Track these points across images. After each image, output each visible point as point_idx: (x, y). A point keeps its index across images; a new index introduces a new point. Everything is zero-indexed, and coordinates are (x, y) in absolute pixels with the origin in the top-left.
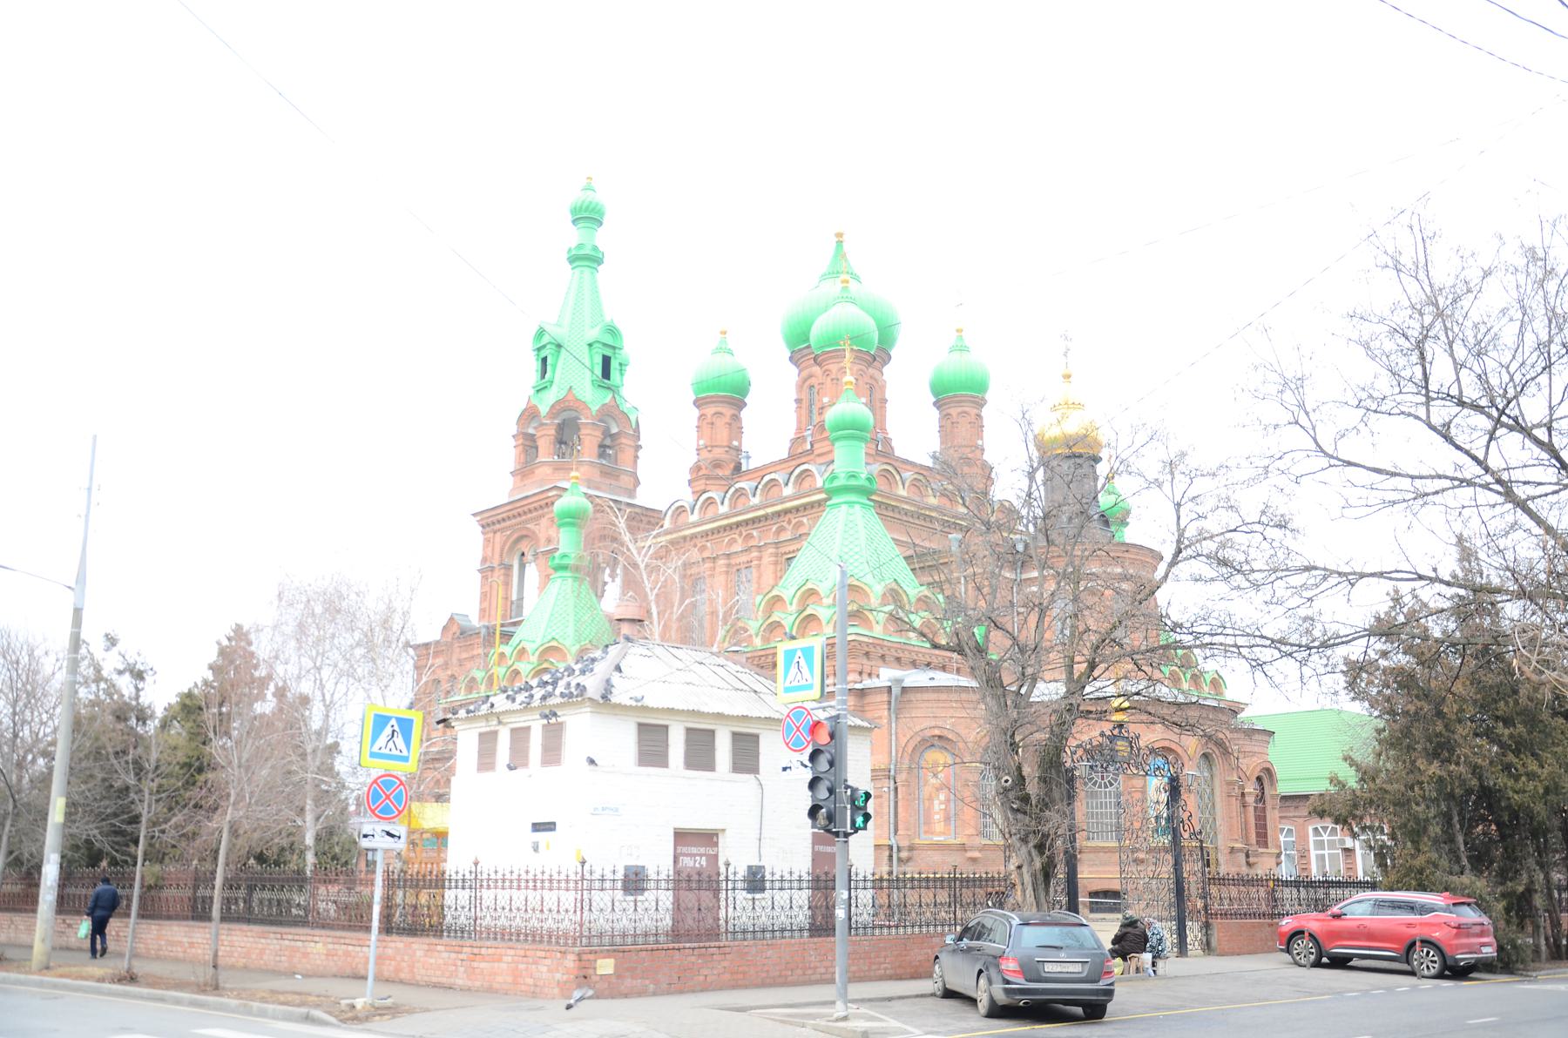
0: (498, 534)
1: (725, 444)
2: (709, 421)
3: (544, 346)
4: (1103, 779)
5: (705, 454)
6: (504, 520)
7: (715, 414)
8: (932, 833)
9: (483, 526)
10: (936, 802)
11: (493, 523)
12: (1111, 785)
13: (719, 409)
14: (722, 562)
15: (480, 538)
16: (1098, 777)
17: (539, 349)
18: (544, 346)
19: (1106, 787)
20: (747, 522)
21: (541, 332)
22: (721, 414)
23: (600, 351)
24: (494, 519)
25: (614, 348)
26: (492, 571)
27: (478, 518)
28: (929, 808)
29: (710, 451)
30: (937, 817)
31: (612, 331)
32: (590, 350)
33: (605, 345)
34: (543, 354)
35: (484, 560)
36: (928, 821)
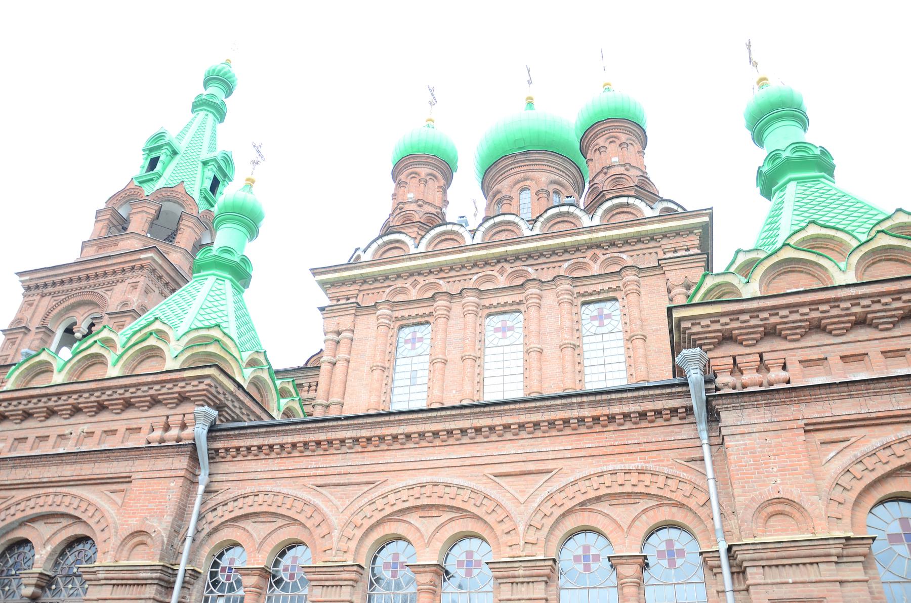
0: (47, 298)
3: (160, 147)
6: (62, 282)
7: (430, 174)
9: (28, 288)
11: (46, 285)
13: (435, 172)
14: (471, 299)
15: (20, 299)
17: (151, 150)
18: (160, 147)
20: (517, 257)
21: (160, 136)
22: (436, 177)
23: (215, 169)
24: (49, 281)
25: (225, 175)
26: (25, 334)
27: (27, 278)
29: (420, 206)
31: (227, 159)
32: (203, 168)
33: (220, 168)
34: (154, 155)
35: (18, 320)
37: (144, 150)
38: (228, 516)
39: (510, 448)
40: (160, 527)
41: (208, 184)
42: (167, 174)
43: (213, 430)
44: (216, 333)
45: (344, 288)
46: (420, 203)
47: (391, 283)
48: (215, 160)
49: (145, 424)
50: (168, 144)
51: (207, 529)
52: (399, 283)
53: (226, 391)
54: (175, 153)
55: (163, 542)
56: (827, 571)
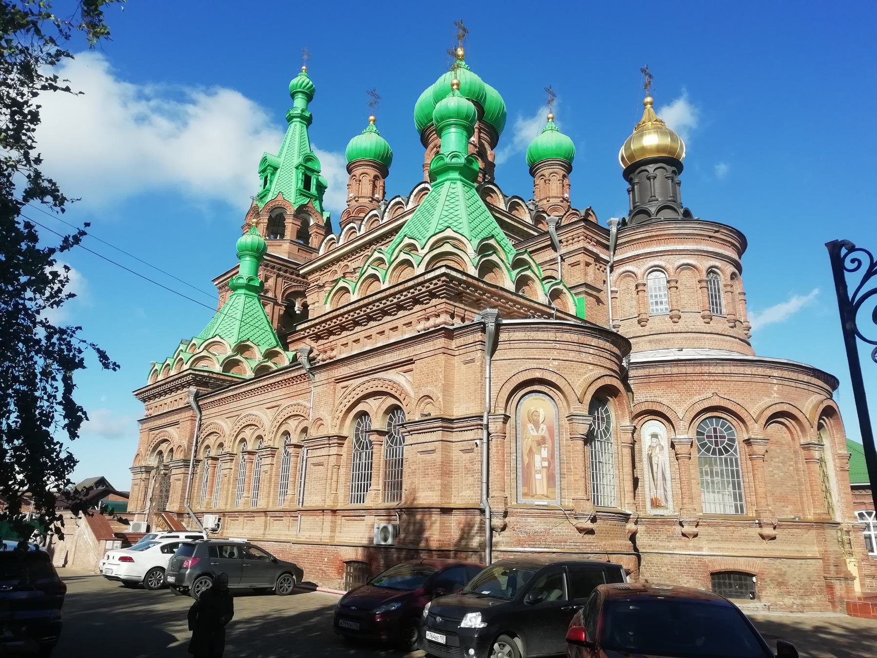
1: (369, 195)
2: (357, 178)
4: (717, 445)
5: (353, 203)
8: (533, 496)
10: (537, 458)
12: (714, 453)
16: (711, 442)
17: (264, 171)
19: (721, 453)
21: (265, 160)
28: (529, 464)
29: (357, 201)
30: (538, 476)
34: (265, 175)
36: (527, 480)
37: (260, 173)
38: (206, 434)
39: (270, 395)
40: (185, 443)
41: (301, 185)
42: (272, 190)
43: (197, 396)
44: (217, 339)
45: (314, 275)
46: (357, 199)
47: (331, 268)
48: (301, 165)
49: (183, 396)
50: (269, 165)
51: (201, 440)
52: (334, 268)
53: (204, 377)
54: (276, 169)
55: (185, 450)
56: (324, 451)
